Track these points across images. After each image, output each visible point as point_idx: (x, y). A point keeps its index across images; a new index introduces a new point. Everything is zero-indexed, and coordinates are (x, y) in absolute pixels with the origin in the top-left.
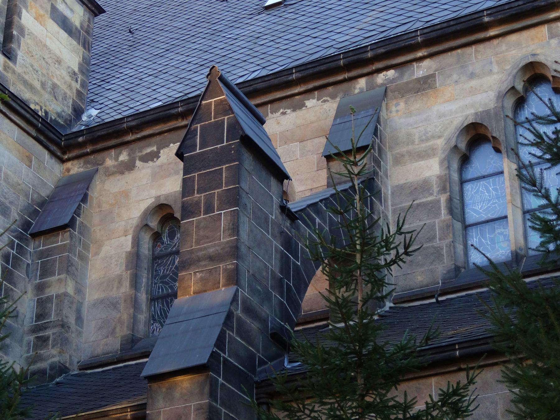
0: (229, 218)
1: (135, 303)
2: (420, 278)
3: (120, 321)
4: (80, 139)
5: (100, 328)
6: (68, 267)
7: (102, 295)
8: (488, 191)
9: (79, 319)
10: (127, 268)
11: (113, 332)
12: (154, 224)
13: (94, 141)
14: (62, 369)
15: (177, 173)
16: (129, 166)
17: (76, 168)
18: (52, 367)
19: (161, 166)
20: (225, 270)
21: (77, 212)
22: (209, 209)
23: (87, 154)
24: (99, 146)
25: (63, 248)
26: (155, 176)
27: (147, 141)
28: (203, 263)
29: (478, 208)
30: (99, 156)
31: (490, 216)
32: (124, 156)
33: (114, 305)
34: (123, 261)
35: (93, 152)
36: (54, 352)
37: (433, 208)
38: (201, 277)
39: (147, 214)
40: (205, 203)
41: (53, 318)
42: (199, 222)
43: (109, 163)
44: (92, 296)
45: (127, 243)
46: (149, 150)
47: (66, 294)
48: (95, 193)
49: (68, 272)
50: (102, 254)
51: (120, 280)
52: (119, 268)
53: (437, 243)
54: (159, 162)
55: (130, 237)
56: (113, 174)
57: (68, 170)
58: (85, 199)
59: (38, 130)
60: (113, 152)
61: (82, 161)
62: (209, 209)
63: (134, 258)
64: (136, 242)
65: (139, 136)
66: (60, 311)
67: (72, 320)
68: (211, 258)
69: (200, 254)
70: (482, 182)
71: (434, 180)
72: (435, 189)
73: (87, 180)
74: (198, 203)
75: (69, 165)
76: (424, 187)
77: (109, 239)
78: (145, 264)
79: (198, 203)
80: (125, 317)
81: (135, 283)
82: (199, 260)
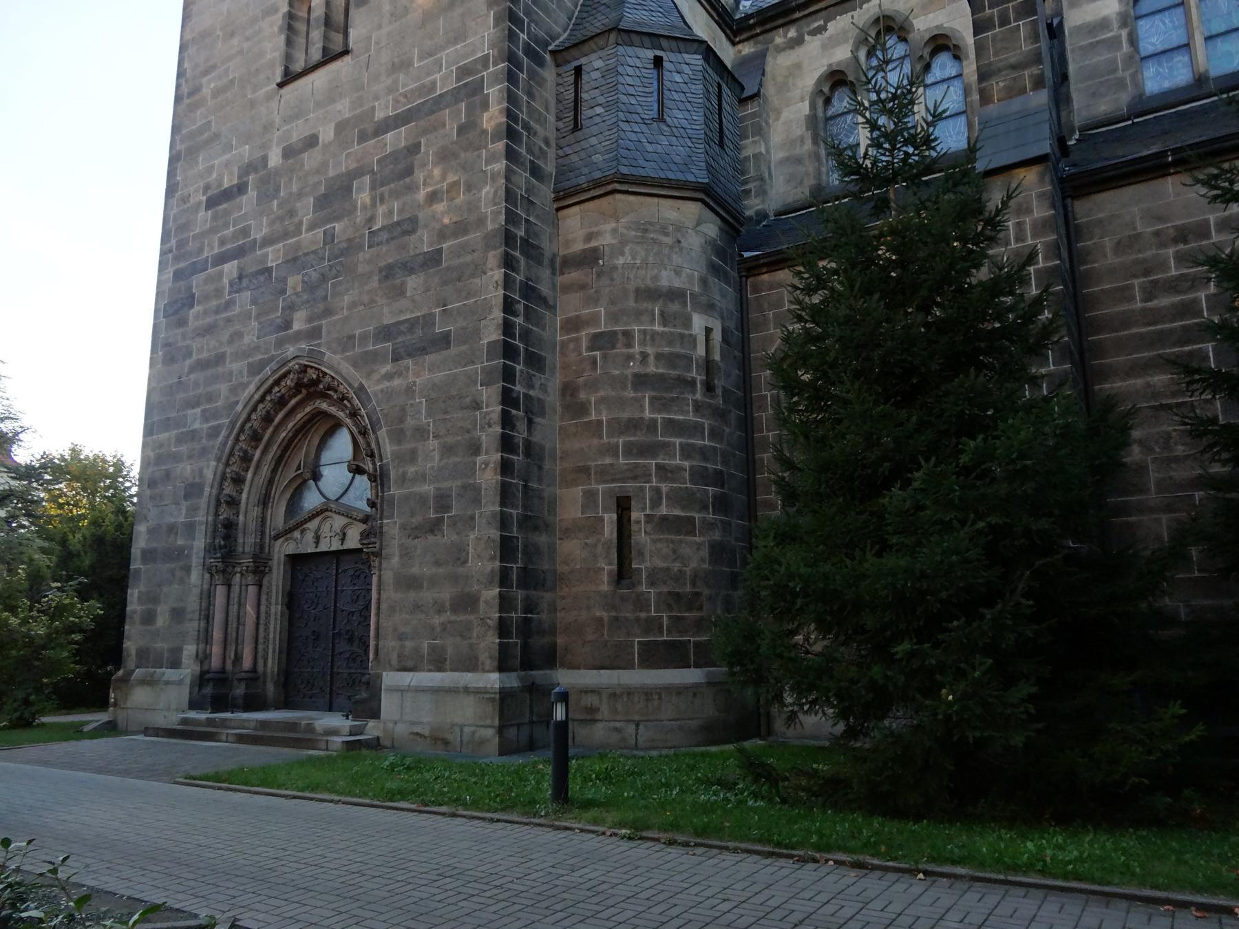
0: (1029, 27)
1: (817, 156)
2: (1103, 108)
3: (807, 174)
4: (751, 22)
5: (789, 181)
6: (760, 131)
7: (787, 154)
8: (1164, 23)
9: (770, 174)
10: (807, 129)
11: (801, 182)
12: (826, 90)
13: (761, 23)
14: (762, 215)
15: (846, 41)
16: (799, 41)
17: (747, 49)
18: (758, 213)
19: (830, 38)
20: (1031, 76)
21: (761, 85)
22: (1004, 21)
23: (757, 35)
24: (768, 26)
25: (754, 115)
26: (824, 47)
27: (814, 17)
28: (1004, 73)
29: (1154, 40)
30: (770, 34)
31: (1166, 47)
32: (792, 33)
33: (798, 160)
34: (804, 123)
35: (762, 33)
36: (757, 201)
37: (1114, 43)
38: (1004, 87)
39: (820, 81)
40: (999, 18)
41: (752, 174)
42: (994, 37)
43: (779, 40)
44: (777, 155)
45: (805, 108)
46: (816, 25)
47: (760, 153)
48: (768, 69)
49: (760, 134)
50: (782, 120)
51: (802, 139)
52: (799, 130)
53: (1120, 73)
54: (827, 34)
55: (807, 103)
56: (784, 49)
57: (740, 52)
58: (763, 75)
59: (719, 14)
60: (781, 31)
61: (752, 42)
62: (1004, 21)
63: (812, 121)
64: (813, 106)
65: (806, 12)
66: (758, 167)
67: (766, 175)
68: (1014, 67)
69: (1000, 65)
70: (1157, 17)
71: (1114, 16)
72: (1115, 25)
73: (761, 57)
74: (991, 19)
75: (740, 47)
76: (1104, 24)
77: (788, 106)
78: (821, 125)
79: (991, 19)
80: (811, 169)
81: (815, 140)
82: (1000, 70)
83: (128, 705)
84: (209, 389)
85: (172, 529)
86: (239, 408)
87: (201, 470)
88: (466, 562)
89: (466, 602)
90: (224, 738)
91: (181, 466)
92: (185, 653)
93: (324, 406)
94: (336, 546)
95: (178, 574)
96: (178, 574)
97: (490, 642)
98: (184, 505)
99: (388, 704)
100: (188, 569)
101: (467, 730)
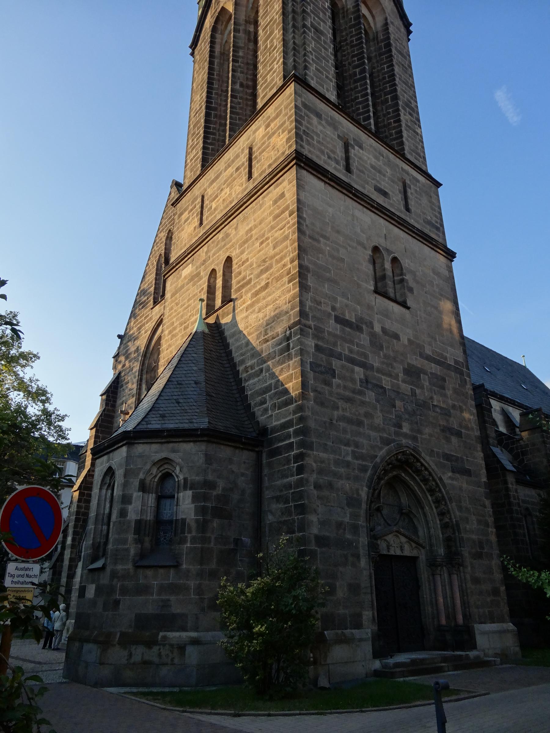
83: (329, 661)
84: (356, 439)
85: (339, 525)
86: (378, 460)
87: (357, 490)
88: (493, 574)
89: (495, 592)
90: (446, 669)
91: (341, 482)
92: (364, 617)
93: (403, 475)
94: (399, 553)
95: (351, 559)
96: (351, 559)
97: (506, 609)
98: (348, 511)
99: (480, 640)
100: (358, 557)
101: (512, 648)
